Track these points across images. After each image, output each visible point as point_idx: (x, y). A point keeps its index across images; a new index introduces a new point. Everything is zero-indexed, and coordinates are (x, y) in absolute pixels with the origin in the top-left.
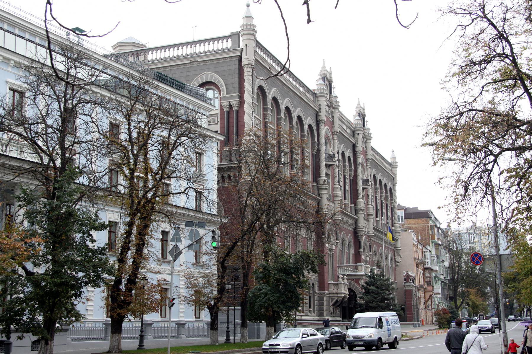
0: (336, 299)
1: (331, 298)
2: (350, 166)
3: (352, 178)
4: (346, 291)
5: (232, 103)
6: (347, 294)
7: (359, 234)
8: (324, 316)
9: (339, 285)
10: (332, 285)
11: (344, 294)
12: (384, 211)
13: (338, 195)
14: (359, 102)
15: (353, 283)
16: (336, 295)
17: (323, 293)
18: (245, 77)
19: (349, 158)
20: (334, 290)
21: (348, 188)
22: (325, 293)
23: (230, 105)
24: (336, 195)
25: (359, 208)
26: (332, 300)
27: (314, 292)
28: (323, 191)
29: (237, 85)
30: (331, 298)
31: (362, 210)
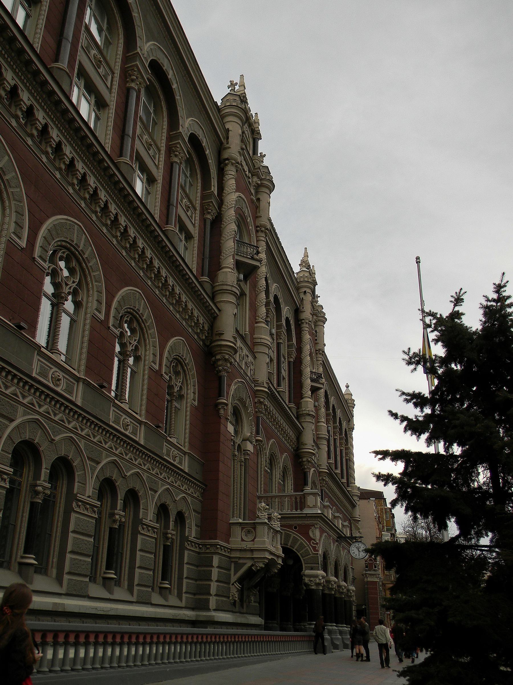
0: (249, 564)
1: (236, 563)
2: (290, 339)
3: (292, 360)
4: (277, 549)
6: (278, 557)
7: (304, 459)
8: (208, 610)
9: (259, 528)
10: (237, 530)
11: (271, 553)
13: (263, 341)
15: (294, 534)
16: (249, 555)
17: (212, 545)
19: (287, 320)
20: (243, 540)
21: (284, 373)
22: (215, 545)
24: (259, 341)
25: (304, 412)
26: (238, 566)
27: (184, 539)
28: (225, 295)
30: (236, 563)
31: (309, 415)
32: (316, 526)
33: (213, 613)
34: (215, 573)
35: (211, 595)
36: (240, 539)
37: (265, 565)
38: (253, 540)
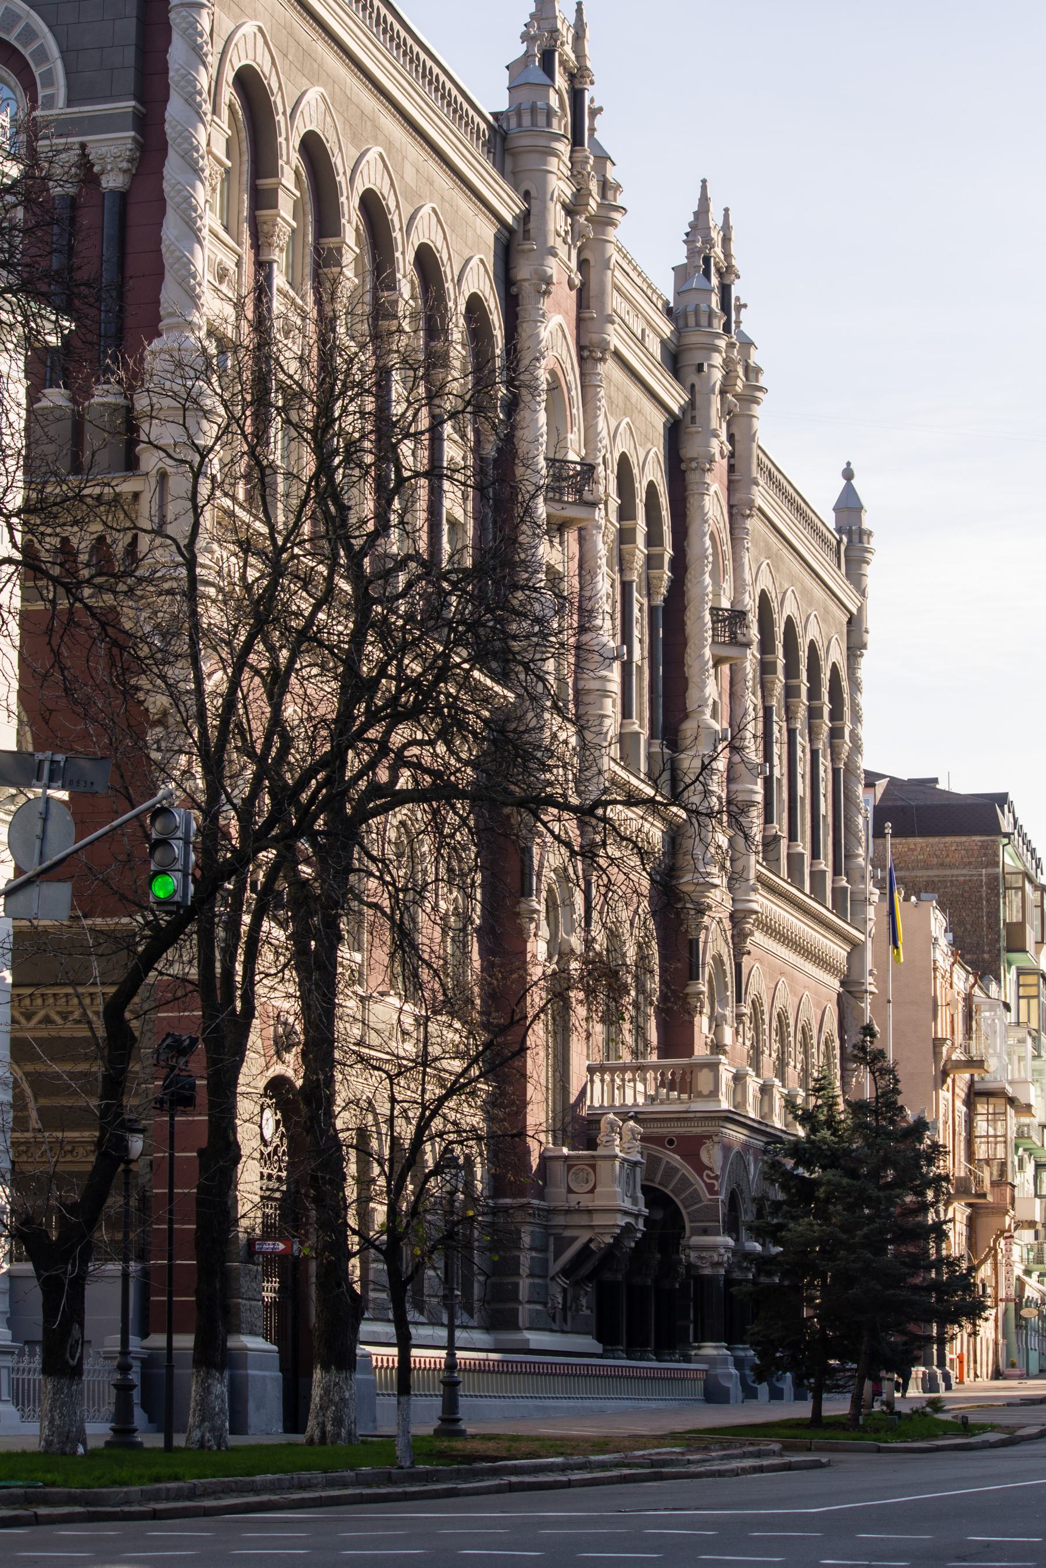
0: (584, 1237)
1: (558, 1238)
2: (653, 539)
4: (635, 1202)
5: (93, 154)
6: (636, 1216)
8: (518, 1329)
11: (626, 1213)
12: (803, 789)
14: (704, 200)
18: (172, 16)
20: (570, 1191)
23: (85, 162)
26: (562, 1244)
29: (130, 56)
32: (716, 1139)
33: (528, 1335)
34: (526, 1260)
35: (520, 1303)
36: (564, 1190)
37: (615, 1238)
38: (592, 1191)
